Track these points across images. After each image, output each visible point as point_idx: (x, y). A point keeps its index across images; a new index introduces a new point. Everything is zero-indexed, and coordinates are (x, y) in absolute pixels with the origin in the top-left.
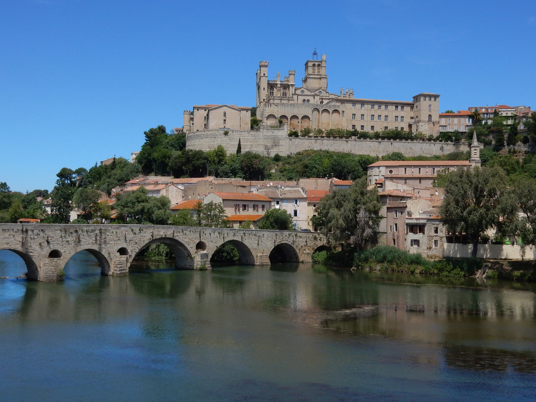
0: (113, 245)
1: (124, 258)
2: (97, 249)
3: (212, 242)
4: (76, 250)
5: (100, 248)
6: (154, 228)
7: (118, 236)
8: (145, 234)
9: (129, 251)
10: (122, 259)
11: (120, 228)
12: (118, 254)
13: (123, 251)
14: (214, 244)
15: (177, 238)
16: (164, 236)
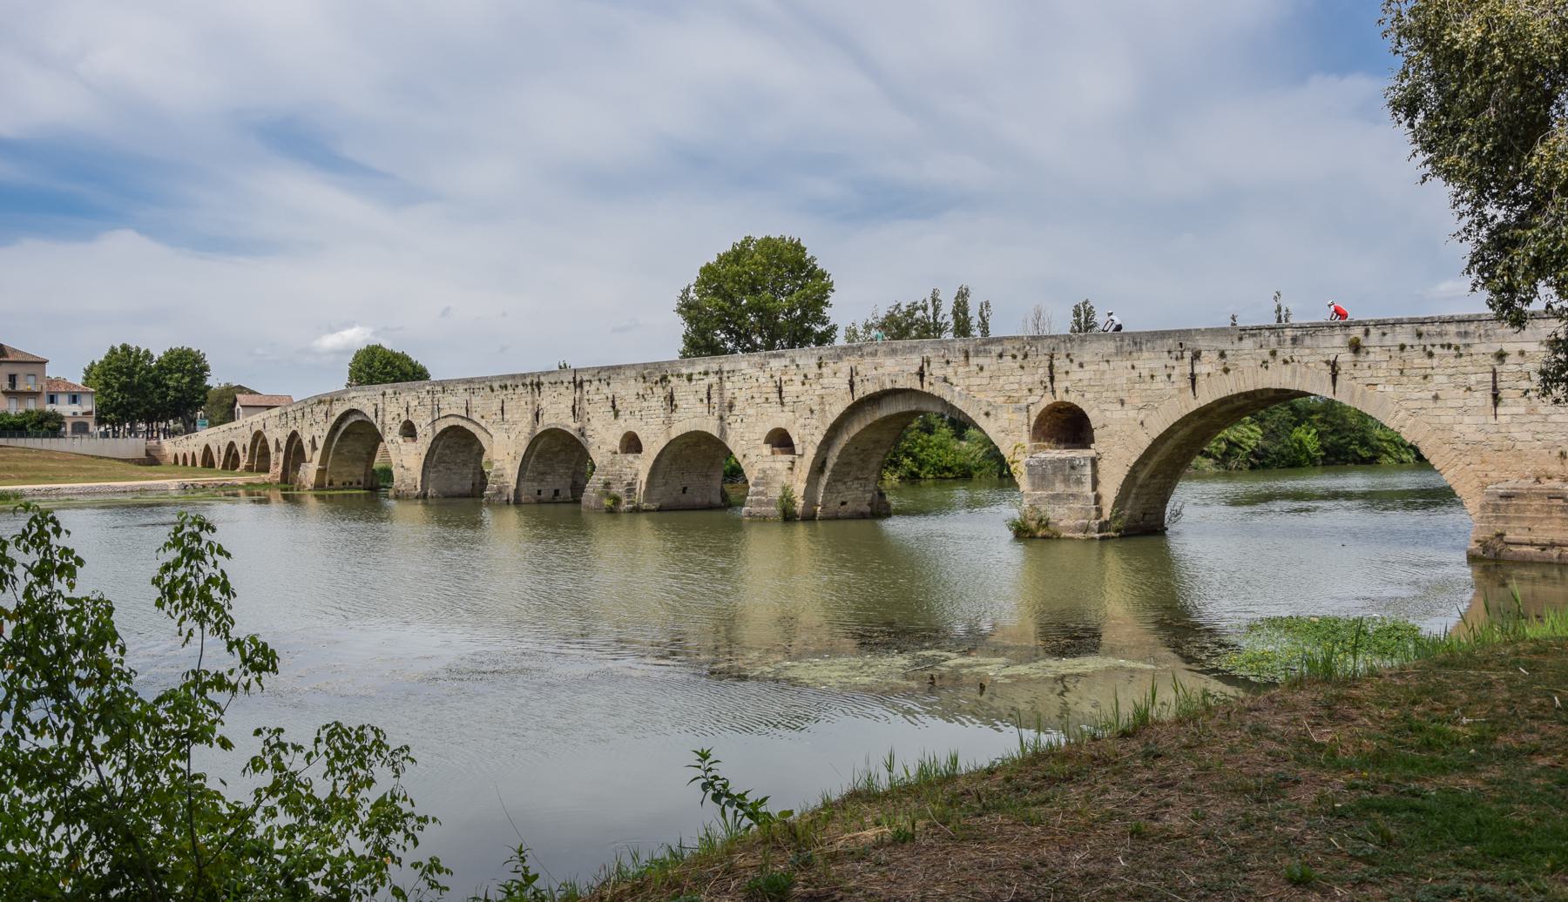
0: (753, 419)
1: (782, 461)
2: (716, 433)
3: (1122, 403)
4: (669, 434)
5: (723, 431)
6: (862, 356)
7: (764, 390)
8: (835, 380)
9: (795, 440)
10: (779, 466)
11: (768, 363)
12: (767, 449)
13: (781, 441)
14: (1132, 414)
15: (938, 390)
16: (888, 386)
